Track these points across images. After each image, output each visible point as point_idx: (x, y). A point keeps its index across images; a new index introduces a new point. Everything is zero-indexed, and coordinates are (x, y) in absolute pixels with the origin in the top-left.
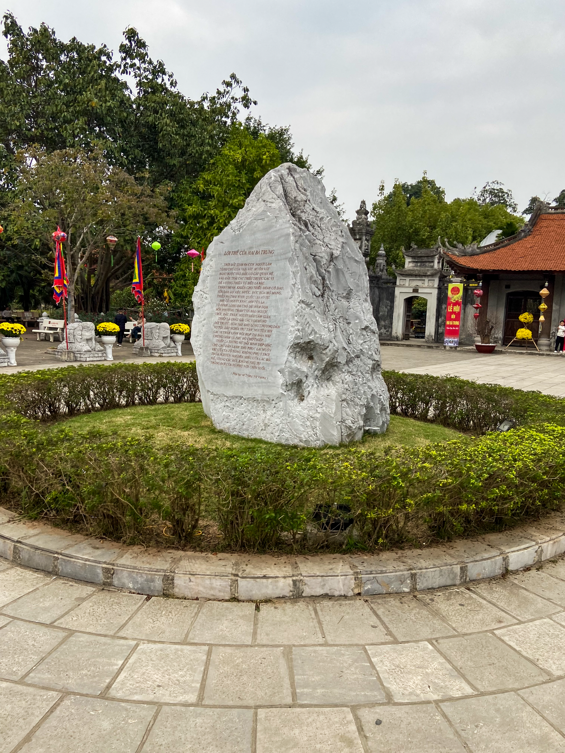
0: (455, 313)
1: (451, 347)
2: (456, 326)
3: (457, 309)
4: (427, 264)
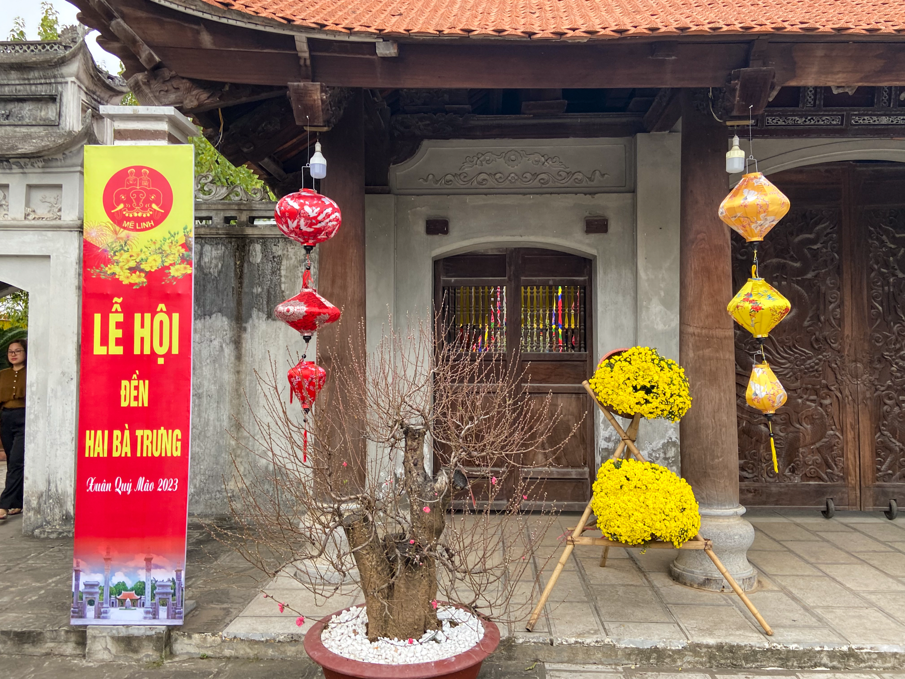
0: (145, 365)
1: (129, 642)
2: (155, 467)
3: (156, 333)
4: (27, 110)
